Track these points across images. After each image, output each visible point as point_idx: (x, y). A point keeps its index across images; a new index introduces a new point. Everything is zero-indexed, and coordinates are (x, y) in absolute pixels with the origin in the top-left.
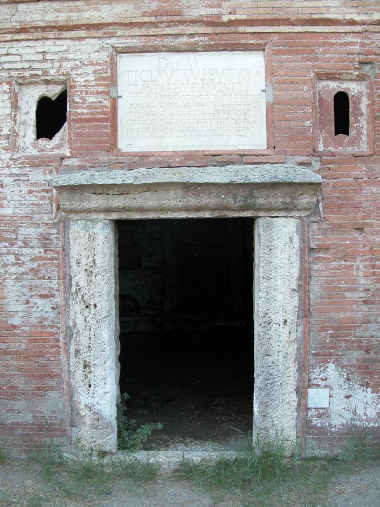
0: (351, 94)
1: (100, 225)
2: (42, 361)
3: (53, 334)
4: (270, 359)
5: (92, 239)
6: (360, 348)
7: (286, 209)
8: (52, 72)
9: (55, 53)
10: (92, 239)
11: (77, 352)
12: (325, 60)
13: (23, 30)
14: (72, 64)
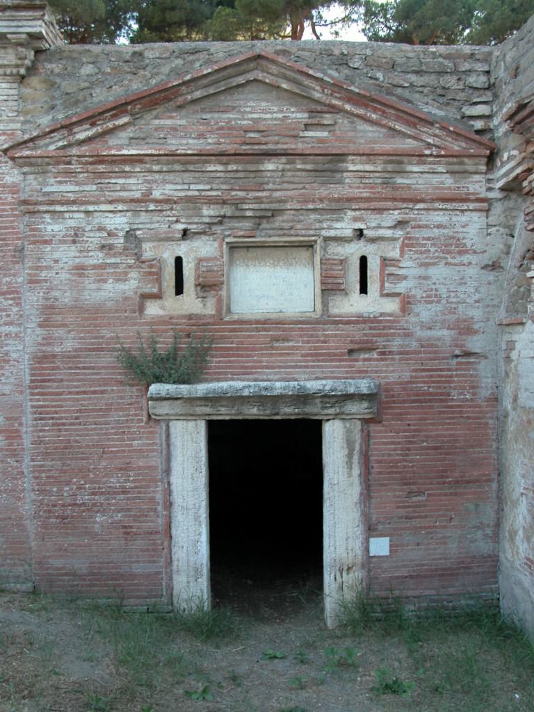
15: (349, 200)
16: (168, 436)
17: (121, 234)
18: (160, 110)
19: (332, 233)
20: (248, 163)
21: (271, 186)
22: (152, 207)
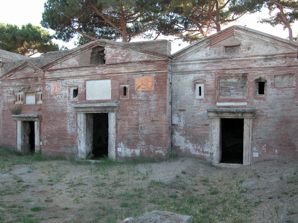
0: (126, 87)
1: (82, 114)
2: (73, 140)
3: (75, 135)
4: (110, 141)
5: (81, 117)
6: (127, 140)
7: (112, 111)
8: (75, 85)
9: (75, 81)
10: (81, 117)
11: (78, 138)
12: (121, 81)
13: (70, 77)
14: (78, 83)
15: (38, 85)
16: (17, 123)
17: (12, 91)
18: (17, 71)
19: (37, 90)
20: (149, 54)
21: (30, 83)
22: (15, 87)
